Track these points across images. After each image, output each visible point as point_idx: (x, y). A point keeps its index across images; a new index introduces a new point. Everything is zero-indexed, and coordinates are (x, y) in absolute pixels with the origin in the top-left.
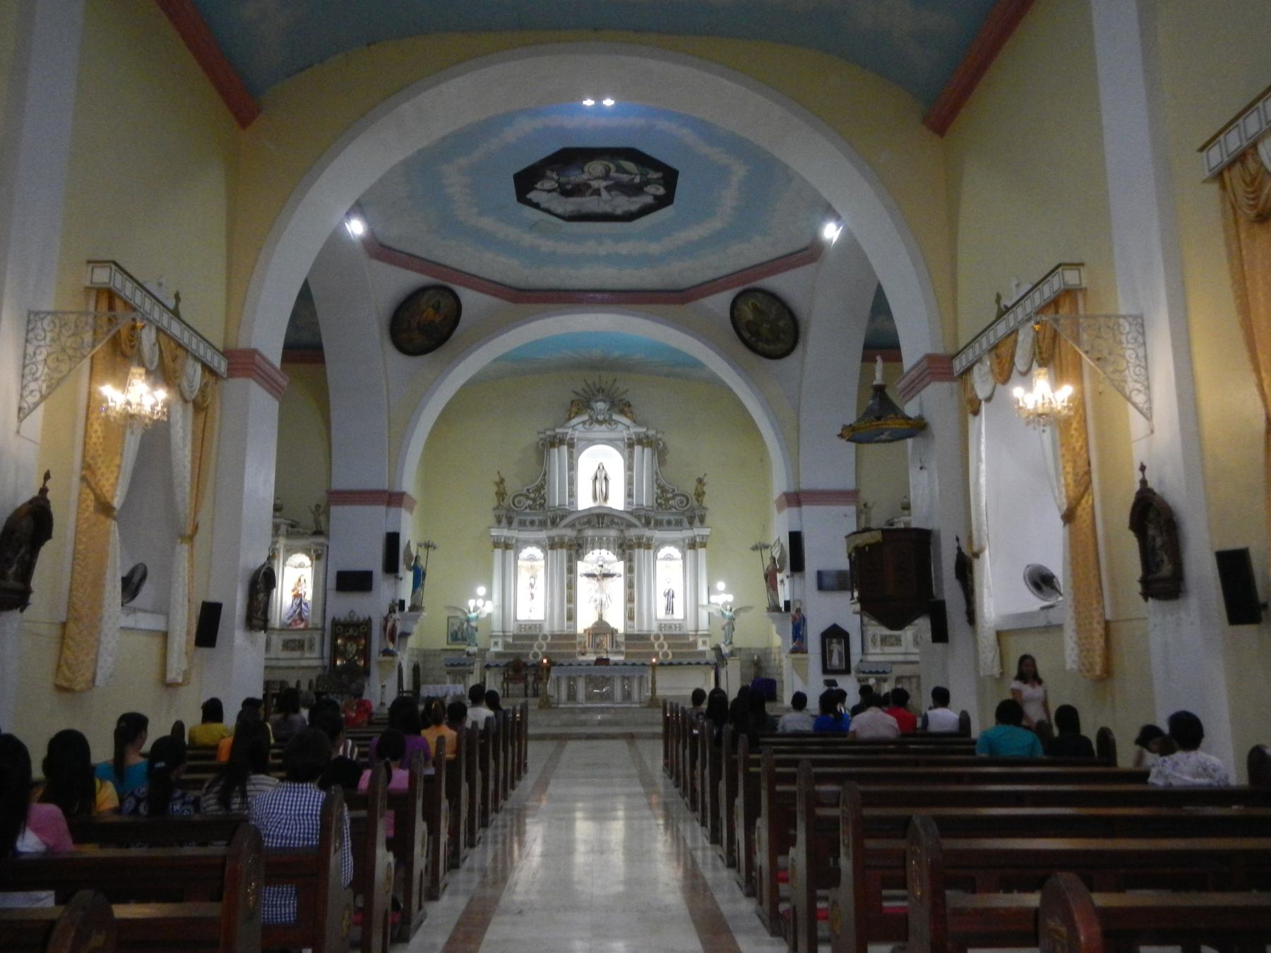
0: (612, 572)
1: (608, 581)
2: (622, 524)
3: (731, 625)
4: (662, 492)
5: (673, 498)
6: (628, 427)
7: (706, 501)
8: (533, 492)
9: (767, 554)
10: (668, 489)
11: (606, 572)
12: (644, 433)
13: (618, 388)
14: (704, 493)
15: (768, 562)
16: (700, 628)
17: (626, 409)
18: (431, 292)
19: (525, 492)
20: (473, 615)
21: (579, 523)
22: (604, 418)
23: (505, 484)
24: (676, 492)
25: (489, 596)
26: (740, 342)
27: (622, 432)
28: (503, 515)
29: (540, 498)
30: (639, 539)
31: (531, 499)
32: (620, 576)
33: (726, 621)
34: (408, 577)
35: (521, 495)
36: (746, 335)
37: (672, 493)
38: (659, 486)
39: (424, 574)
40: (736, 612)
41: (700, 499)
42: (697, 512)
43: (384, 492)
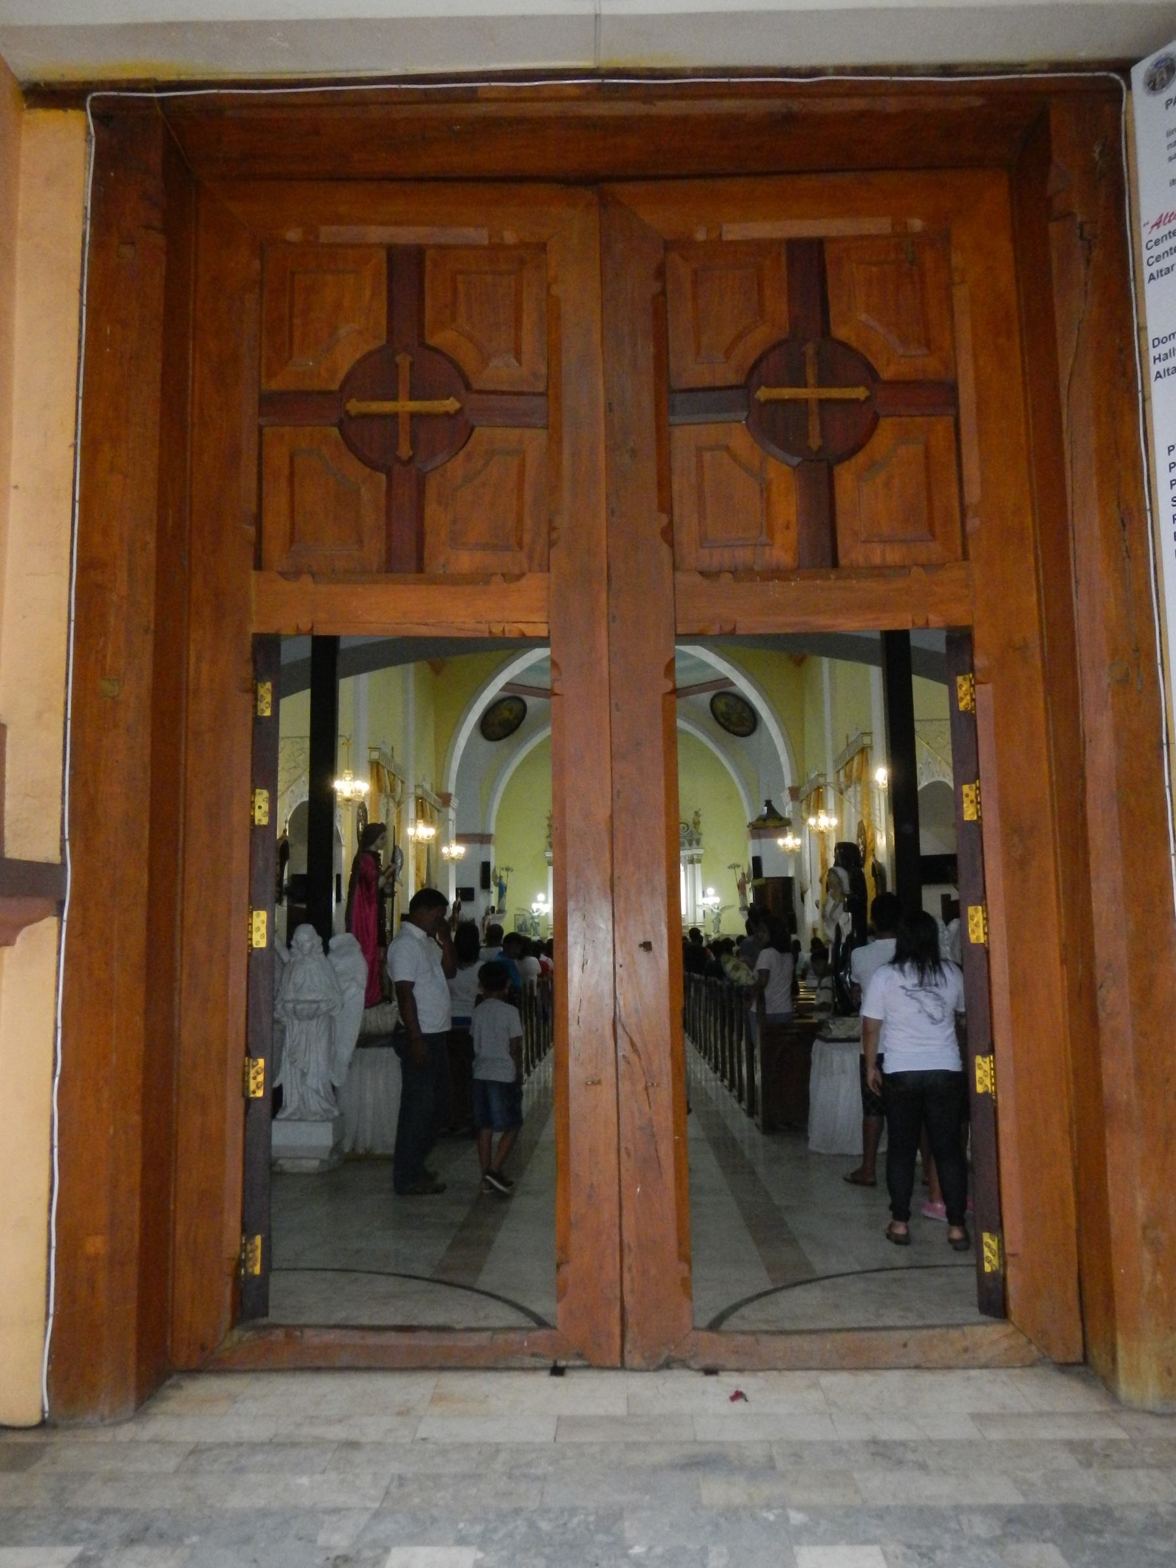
3: (718, 920)
7: (703, 828)
9: (740, 869)
14: (699, 822)
15: (739, 876)
16: (698, 921)
18: (508, 701)
20: (536, 914)
25: (546, 902)
26: (719, 726)
33: (714, 916)
34: (494, 889)
36: (722, 720)
39: (506, 888)
40: (721, 910)
42: (696, 837)
43: (479, 835)
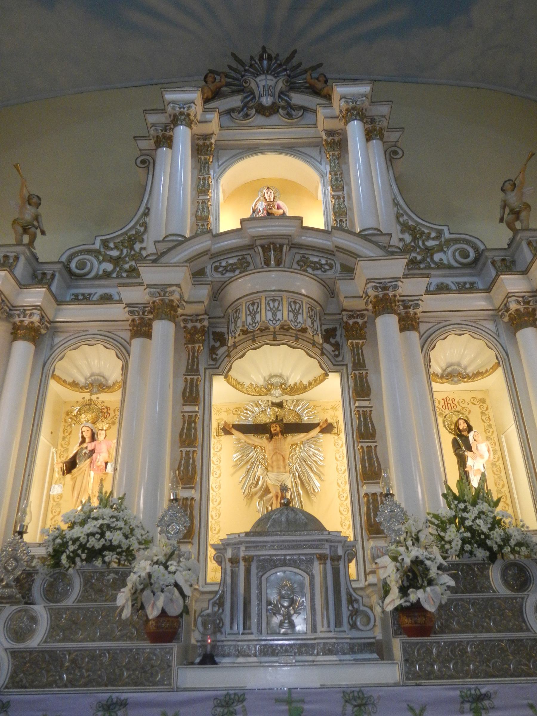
0: (305, 419)
1: (301, 437)
2: (331, 267)
4: (414, 239)
5: (440, 249)
6: (331, 106)
8: (116, 247)
10: (426, 231)
11: (290, 419)
12: (365, 96)
13: (300, 64)
17: (319, 85)
19: (97, 245)
21: (216, 269)
22: (274, 104)
23: (41, 210)
24: (447, 235)
27: (315, 125)
28: (17, 258)
29: (133, 258)
30: (385, 288)
31: (111, 260)
32: (328, 428)
35: (88, 252)
37: (437, 238)
38: (405, 228)
41: (518, 225)
